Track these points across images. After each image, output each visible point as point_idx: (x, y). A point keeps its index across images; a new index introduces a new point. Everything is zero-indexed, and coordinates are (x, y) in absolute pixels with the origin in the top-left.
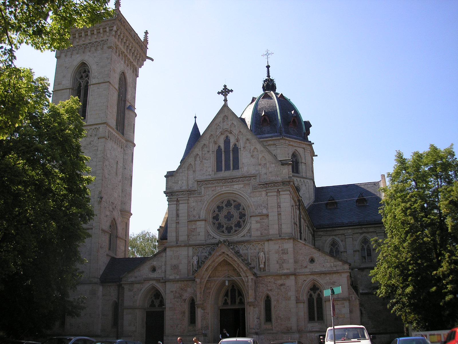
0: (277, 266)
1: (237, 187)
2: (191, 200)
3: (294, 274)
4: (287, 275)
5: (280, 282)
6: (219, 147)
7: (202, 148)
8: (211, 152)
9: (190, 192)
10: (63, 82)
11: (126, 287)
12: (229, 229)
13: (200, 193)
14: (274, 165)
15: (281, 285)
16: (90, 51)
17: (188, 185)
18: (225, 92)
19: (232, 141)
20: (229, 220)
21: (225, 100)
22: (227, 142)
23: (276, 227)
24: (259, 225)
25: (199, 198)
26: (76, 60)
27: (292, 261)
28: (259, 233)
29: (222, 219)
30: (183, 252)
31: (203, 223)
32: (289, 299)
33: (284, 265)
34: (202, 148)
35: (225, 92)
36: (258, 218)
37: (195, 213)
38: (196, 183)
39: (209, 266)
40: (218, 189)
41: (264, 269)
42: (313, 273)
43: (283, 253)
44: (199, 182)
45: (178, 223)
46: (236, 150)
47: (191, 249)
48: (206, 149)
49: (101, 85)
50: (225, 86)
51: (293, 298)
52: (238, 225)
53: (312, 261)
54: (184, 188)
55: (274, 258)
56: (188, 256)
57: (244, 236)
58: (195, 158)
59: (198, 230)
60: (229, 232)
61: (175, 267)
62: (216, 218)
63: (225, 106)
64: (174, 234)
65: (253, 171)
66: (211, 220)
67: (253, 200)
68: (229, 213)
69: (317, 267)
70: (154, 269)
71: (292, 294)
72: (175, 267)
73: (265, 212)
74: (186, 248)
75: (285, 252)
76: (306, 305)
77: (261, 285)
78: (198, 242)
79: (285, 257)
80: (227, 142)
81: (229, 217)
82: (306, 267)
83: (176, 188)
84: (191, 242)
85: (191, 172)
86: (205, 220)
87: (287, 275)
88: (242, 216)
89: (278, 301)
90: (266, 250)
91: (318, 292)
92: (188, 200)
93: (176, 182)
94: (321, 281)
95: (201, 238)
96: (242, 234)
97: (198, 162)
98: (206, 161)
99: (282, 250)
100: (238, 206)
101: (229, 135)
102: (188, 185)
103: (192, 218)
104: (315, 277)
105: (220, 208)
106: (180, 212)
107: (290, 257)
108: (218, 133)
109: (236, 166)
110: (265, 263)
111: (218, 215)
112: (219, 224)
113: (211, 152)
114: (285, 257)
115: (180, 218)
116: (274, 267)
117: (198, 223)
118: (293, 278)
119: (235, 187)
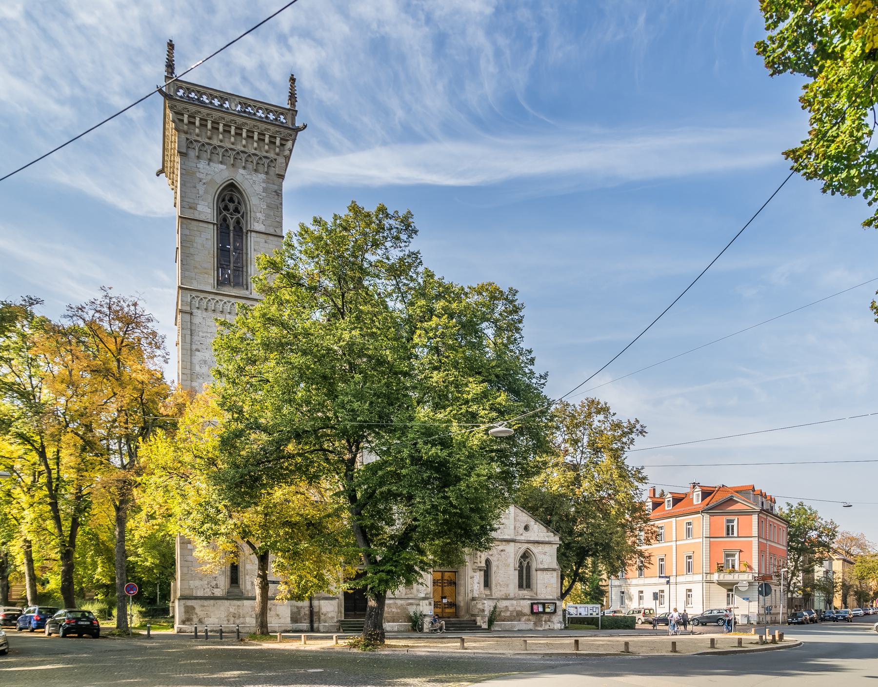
5: (501, 548)
16: (244, 168)
26: (218, 173)
32: (508, 566)
42: (529, 542)
51: (512, 565)
53: (526, 528)
94: (535, 549)
104: (530, 546)
118: (512, 544)
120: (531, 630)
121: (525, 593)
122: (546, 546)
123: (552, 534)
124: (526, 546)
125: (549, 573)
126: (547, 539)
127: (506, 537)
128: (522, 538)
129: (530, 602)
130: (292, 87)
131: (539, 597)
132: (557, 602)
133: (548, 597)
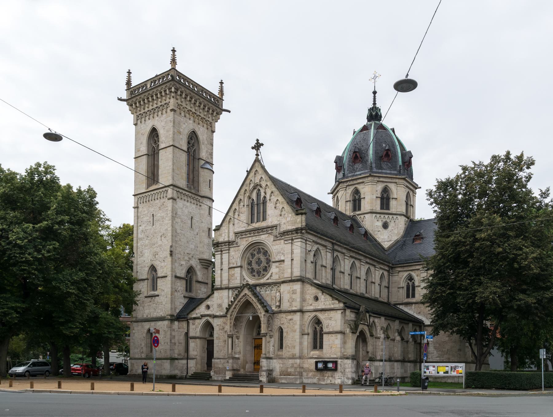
0: (288, 304)
1: (264, 238)
2: (232, 249)
3: (301, 311)
4: (295, 312)
6: (253, 200)
7: (239, 203)
8: (245, 206)
9: (229, 243)
10: (141, 149)
11: (191, 321)
12: (259, 273)
13: (237, 244)
14: (290, 215)
15: (291, 320)
17: (229, 237)
18: (258, 146)
19: (263, 194)
20: (259, 266)
21: (257, 155)
22: (258, 195)
23: (289, 271)
24: (278, 269)
25: (237, 248)
27: (298, 300)
28: (277, 277)
29: (255, 266)
30: (225, 293)
31: (239, 269)
33: (293, 303)
34: (239, 203)
35: (258, 146)
36: (277, 264)
37: (234, 261)
38: (234, 235)
39: (236, 305)
40: (250, 239)
41: (279, 306)
43: (293, 294)
44: (236, 233)
45: (222, 269)
46: (264, 203)
47: (231, 291)
48: (242, 204)
49: (168, 148)
50: (258, 140)
51: (298, 330)
52: (266, 269)
53: (316, 299)
54: (226, 239)
55: (286, 297)
56: (229, 297)
57: (268, 279)
58: (234, 213)
59: (236, 275)
60: (259, 276)
61: (220, 306)
62: (250, 264)
63: (257, 161)
64: (219, 279)
65: (275, 222)
66: (245, 266)
67: (278, 248)
68: (259, 259)
69: (320, 305)
70: (208, 307)
71: (297, 327)
72: (220, 306)
73: (282, 258)
74: (227, 291)
75: (294, 292)
76: (311, 336)
77: (276, 320)
78: (235, 285)
79: (294, 296)
80: (258, 195)
81: (259, 262)
82: (311, 305)
83: (221, 240)
84: (231, 286)
85: (231, 225)
86: (241, 267)
87: (295, 312)
88: (268, 261)
89: (287, 333)
90: (282, 291)
91: (321, 325)
92: (229, 250)
93: (221, 235)
94: (322, 316)
95: (237, 282)
96: (266, 278)
97: (236, 216)
98: (242, 215)
99: (292, 291)
100: (266, 253)
101: (260, 189)
102: (229, 237)
103: (231, 266)
105: (253, 255)
106: (223, 260)
107: (297, 297)
108: (251, 187)
109: (264, 219)
110: (280, 301)
111: (251, 261)
112: (252, 269)
113: (245, 206)
114: (294, 296)
115: (223, 266)
116: (285, 306)
117: (236, 269)
118: (299, 314)
119: (263, 237)
120: (315, 384)
121: (316, 353)
122: (332, 312)
123: (337, 302)
124: (314, 314)
125: (333, 335)
126: (332, 306)
127: (294, 309)
128: (312, 308)
129: (315, 360)
130: (174, 55)
131: (325, 356)
132: (339, 361)
133: (332, 356)
